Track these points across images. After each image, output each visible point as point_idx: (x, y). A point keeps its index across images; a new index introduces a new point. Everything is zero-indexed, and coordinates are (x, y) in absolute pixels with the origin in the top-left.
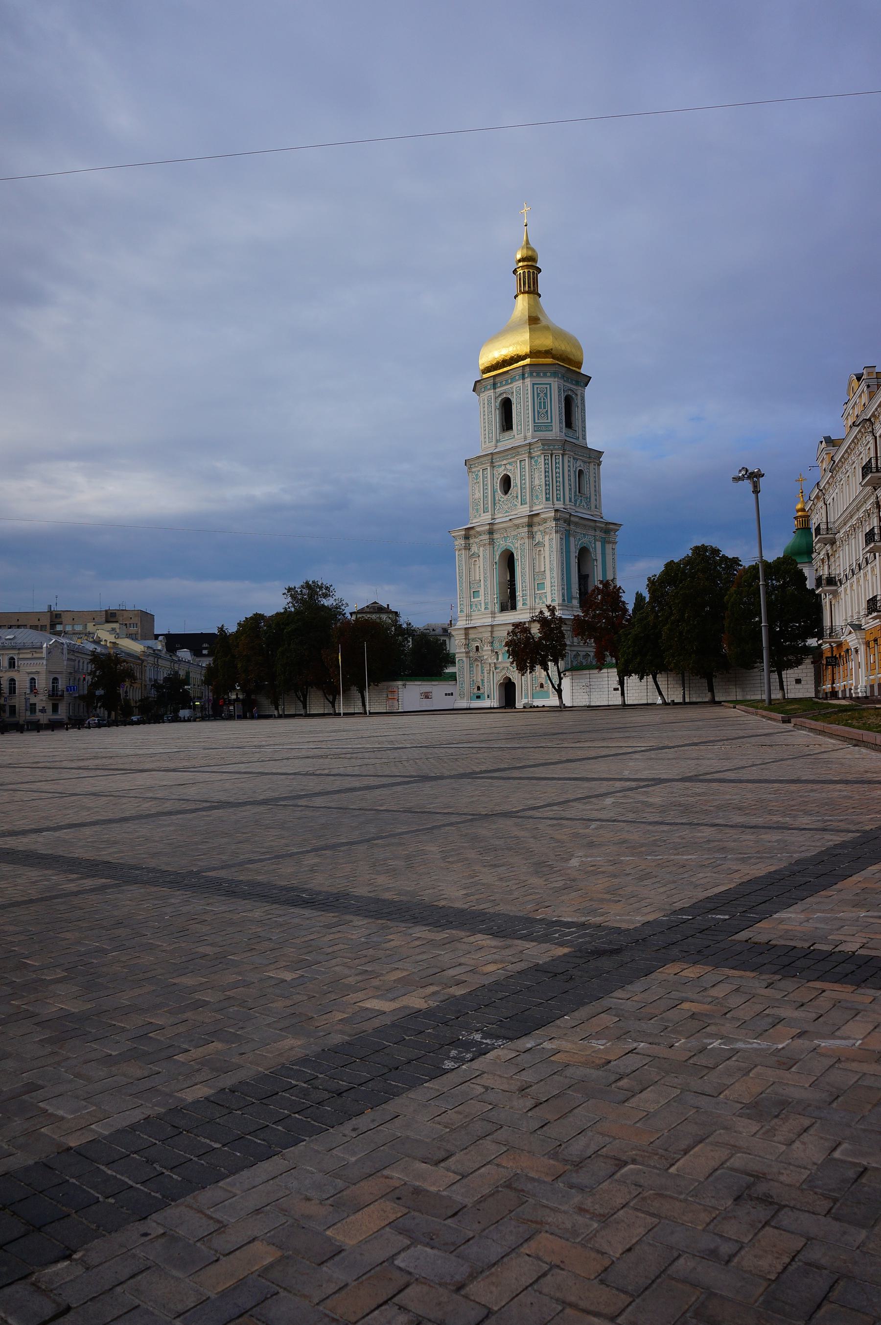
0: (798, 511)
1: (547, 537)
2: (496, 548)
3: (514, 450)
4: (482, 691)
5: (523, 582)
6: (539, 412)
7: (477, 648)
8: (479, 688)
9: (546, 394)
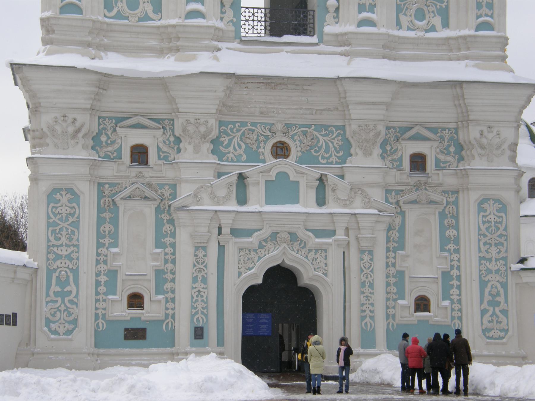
4: (152, 311)
7: (140, 155)
8: (136, 301)
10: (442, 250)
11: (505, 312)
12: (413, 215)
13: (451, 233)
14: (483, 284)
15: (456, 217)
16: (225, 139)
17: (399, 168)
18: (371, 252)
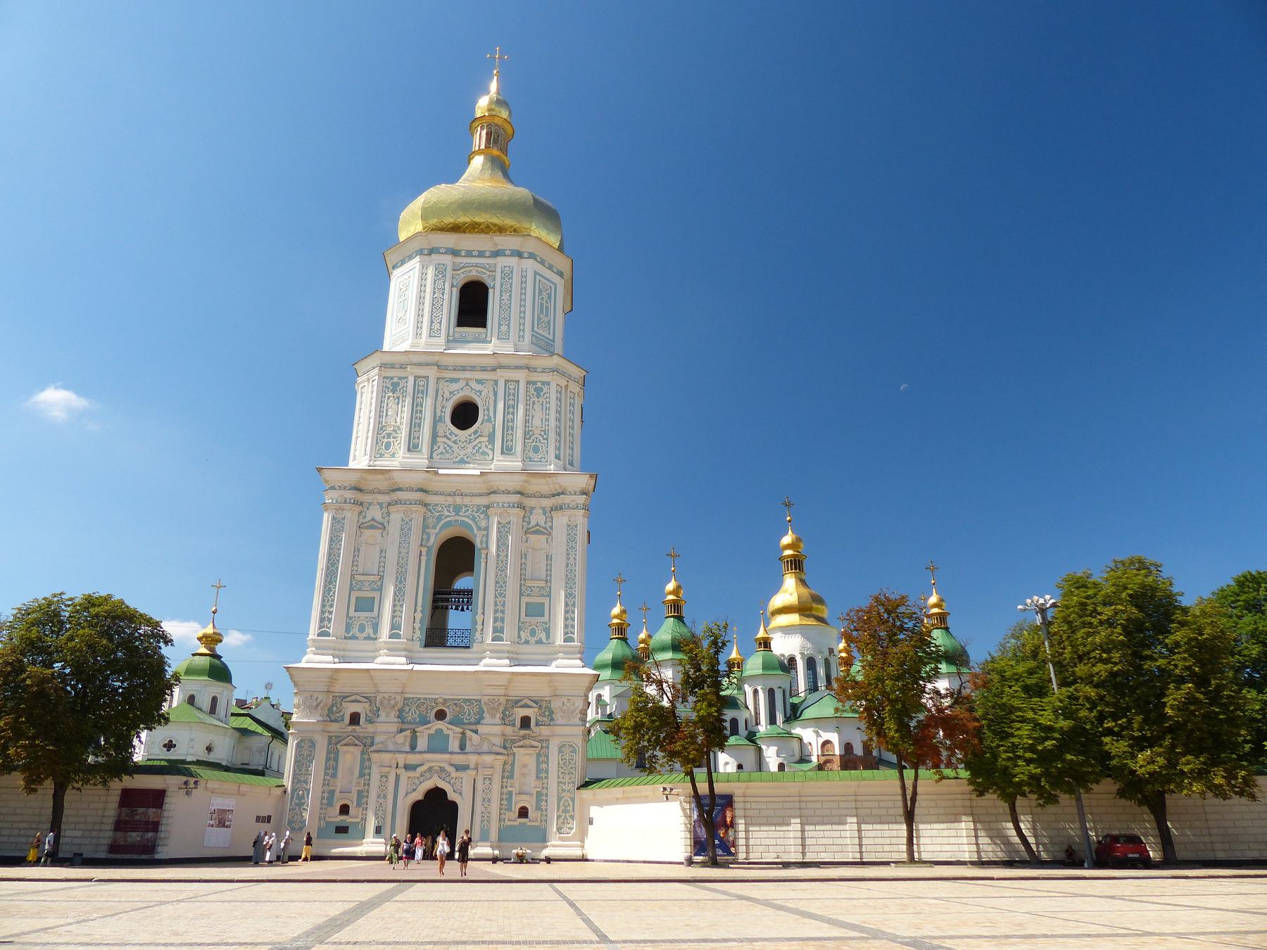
1: (560, 520)
5: (500, 594)
6: (539, 319)
7: (355, 719)
8: (345, 810)
9: (549, 296)
10: (538, 778)
11: (572, 817)
12: (520, 752)
13: (544, 766)
14: (559, 799)
16: (407, 708)
17: (514, 725)
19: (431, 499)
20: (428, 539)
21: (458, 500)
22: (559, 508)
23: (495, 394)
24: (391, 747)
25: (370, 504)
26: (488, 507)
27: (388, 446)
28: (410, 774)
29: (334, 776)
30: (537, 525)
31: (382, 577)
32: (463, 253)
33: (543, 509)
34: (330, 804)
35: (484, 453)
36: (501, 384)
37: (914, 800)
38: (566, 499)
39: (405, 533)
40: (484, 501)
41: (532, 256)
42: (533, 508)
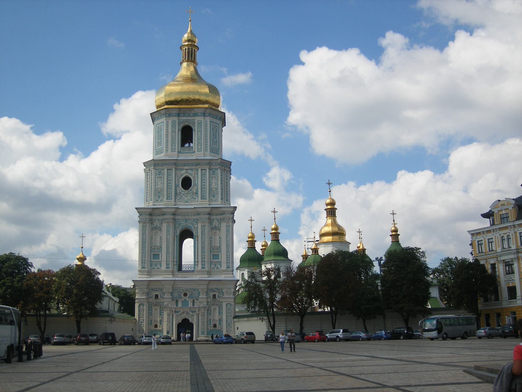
0: (272, 230)
2: (177, 226)
3: (197, 163)
4: (159, 328)
7: (157, 297)
8: (156, 326)
10: (219, 314)
12: (212, 308)
13: (221, 311)
14: (227, 321)
15: (222, 307)
18: (204, 315)
19: (177, 217)
20: (176, 233)
21: (187, 217)
22: (222, 220)
23: (198, 174)
24: (170, 306)
25: (155, 220)
26: (197, 219)
27: (159, 197)
28: (177, 314)
29: (152, 315)
30: (215, 226)
31: (161, 247)
32: (182, 115)
33: (217, 219)
34: (151, 324)
35: (195, 198)
36: (200, 170)
37: (335, 321)
38: (226, 216)
39: (168, 231)
40: (196, 217)
41: (210, 115)
42: (213, 219)
